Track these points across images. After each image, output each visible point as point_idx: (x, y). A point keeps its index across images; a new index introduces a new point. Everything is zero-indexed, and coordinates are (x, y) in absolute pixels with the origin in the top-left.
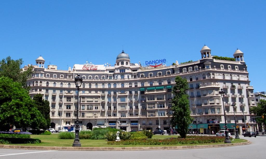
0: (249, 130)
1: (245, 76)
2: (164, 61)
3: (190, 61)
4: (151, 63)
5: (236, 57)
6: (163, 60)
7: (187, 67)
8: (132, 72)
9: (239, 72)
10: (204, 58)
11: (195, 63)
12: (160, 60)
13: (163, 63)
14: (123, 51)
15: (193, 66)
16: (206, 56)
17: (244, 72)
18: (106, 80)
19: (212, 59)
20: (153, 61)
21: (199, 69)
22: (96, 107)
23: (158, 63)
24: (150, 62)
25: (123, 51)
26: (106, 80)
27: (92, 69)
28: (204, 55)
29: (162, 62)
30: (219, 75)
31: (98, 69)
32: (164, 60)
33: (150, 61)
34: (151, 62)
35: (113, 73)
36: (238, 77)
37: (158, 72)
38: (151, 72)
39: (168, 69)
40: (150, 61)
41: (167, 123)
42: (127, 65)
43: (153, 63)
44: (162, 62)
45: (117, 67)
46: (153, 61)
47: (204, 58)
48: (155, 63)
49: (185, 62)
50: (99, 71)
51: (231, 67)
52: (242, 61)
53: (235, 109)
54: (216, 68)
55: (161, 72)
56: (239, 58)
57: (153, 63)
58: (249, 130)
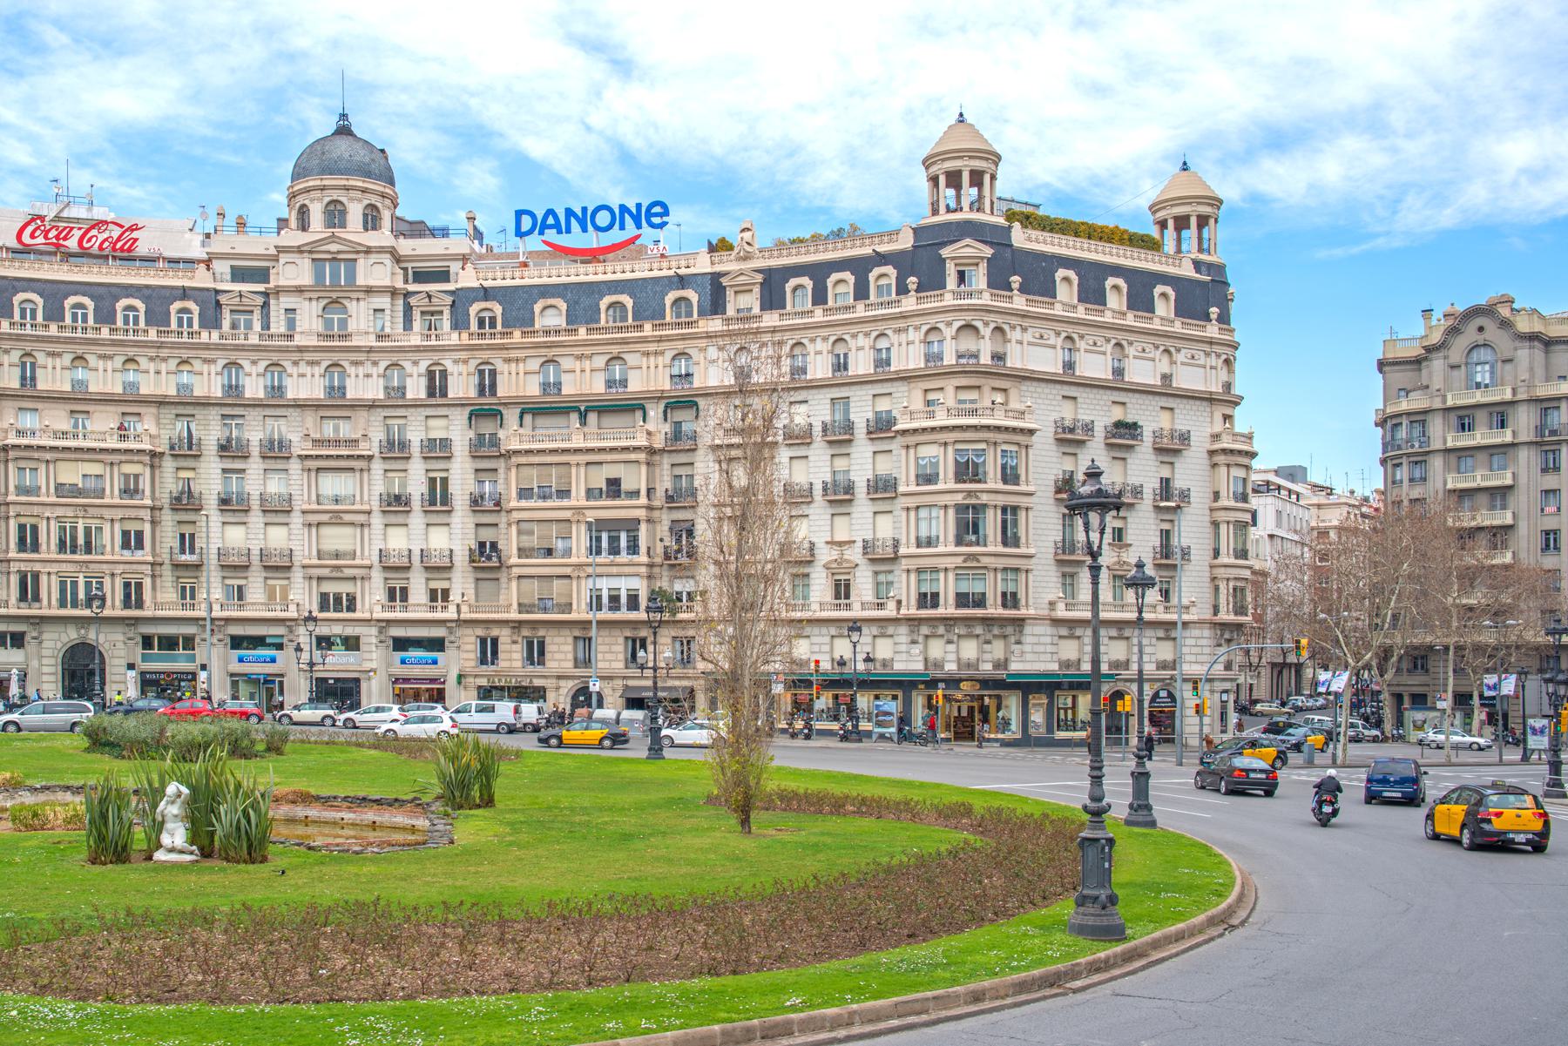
0: (1201, 725)
1: (1213, 361)
2: (656, 220)
3: (840, 230)
4: (557, 226)
5: (1171, 223)
7: (819, 272)
8: (412, 287)
9: (1178, 327)
10: (948, 210)
11: (882, 249)
13: (646, 230)
14: (344, 116)
15: (859, 267)
16: (958, 197)
17: (1212, 330)
18: (205, 335)
19: (1001, 221)
20: (569, 213)
21: (902, 290)
22: (126, 534)
23: (610, 227)
24: (551, 221)
25: (344, 116)
26: (205, 335)
28: (951, 192)
29: (639, 226)
31: (142, 249)
32: (657, 209)
33: (550, 212)
35: (261, 288)
36: (1164, 366)
38: (553, 296)
39: (682, 281)
40: (550, 212)
42: (374, 228)
44: (639, 226)
45: (293, 237)
47: (942, 209)
48: (585, 230)
49: (808, 236)
51: (1125, 290)
52: (1204, 257)
54: (1023, 289)
55: (628, 301)
56: (1185, 233)
58: (1201, 725)
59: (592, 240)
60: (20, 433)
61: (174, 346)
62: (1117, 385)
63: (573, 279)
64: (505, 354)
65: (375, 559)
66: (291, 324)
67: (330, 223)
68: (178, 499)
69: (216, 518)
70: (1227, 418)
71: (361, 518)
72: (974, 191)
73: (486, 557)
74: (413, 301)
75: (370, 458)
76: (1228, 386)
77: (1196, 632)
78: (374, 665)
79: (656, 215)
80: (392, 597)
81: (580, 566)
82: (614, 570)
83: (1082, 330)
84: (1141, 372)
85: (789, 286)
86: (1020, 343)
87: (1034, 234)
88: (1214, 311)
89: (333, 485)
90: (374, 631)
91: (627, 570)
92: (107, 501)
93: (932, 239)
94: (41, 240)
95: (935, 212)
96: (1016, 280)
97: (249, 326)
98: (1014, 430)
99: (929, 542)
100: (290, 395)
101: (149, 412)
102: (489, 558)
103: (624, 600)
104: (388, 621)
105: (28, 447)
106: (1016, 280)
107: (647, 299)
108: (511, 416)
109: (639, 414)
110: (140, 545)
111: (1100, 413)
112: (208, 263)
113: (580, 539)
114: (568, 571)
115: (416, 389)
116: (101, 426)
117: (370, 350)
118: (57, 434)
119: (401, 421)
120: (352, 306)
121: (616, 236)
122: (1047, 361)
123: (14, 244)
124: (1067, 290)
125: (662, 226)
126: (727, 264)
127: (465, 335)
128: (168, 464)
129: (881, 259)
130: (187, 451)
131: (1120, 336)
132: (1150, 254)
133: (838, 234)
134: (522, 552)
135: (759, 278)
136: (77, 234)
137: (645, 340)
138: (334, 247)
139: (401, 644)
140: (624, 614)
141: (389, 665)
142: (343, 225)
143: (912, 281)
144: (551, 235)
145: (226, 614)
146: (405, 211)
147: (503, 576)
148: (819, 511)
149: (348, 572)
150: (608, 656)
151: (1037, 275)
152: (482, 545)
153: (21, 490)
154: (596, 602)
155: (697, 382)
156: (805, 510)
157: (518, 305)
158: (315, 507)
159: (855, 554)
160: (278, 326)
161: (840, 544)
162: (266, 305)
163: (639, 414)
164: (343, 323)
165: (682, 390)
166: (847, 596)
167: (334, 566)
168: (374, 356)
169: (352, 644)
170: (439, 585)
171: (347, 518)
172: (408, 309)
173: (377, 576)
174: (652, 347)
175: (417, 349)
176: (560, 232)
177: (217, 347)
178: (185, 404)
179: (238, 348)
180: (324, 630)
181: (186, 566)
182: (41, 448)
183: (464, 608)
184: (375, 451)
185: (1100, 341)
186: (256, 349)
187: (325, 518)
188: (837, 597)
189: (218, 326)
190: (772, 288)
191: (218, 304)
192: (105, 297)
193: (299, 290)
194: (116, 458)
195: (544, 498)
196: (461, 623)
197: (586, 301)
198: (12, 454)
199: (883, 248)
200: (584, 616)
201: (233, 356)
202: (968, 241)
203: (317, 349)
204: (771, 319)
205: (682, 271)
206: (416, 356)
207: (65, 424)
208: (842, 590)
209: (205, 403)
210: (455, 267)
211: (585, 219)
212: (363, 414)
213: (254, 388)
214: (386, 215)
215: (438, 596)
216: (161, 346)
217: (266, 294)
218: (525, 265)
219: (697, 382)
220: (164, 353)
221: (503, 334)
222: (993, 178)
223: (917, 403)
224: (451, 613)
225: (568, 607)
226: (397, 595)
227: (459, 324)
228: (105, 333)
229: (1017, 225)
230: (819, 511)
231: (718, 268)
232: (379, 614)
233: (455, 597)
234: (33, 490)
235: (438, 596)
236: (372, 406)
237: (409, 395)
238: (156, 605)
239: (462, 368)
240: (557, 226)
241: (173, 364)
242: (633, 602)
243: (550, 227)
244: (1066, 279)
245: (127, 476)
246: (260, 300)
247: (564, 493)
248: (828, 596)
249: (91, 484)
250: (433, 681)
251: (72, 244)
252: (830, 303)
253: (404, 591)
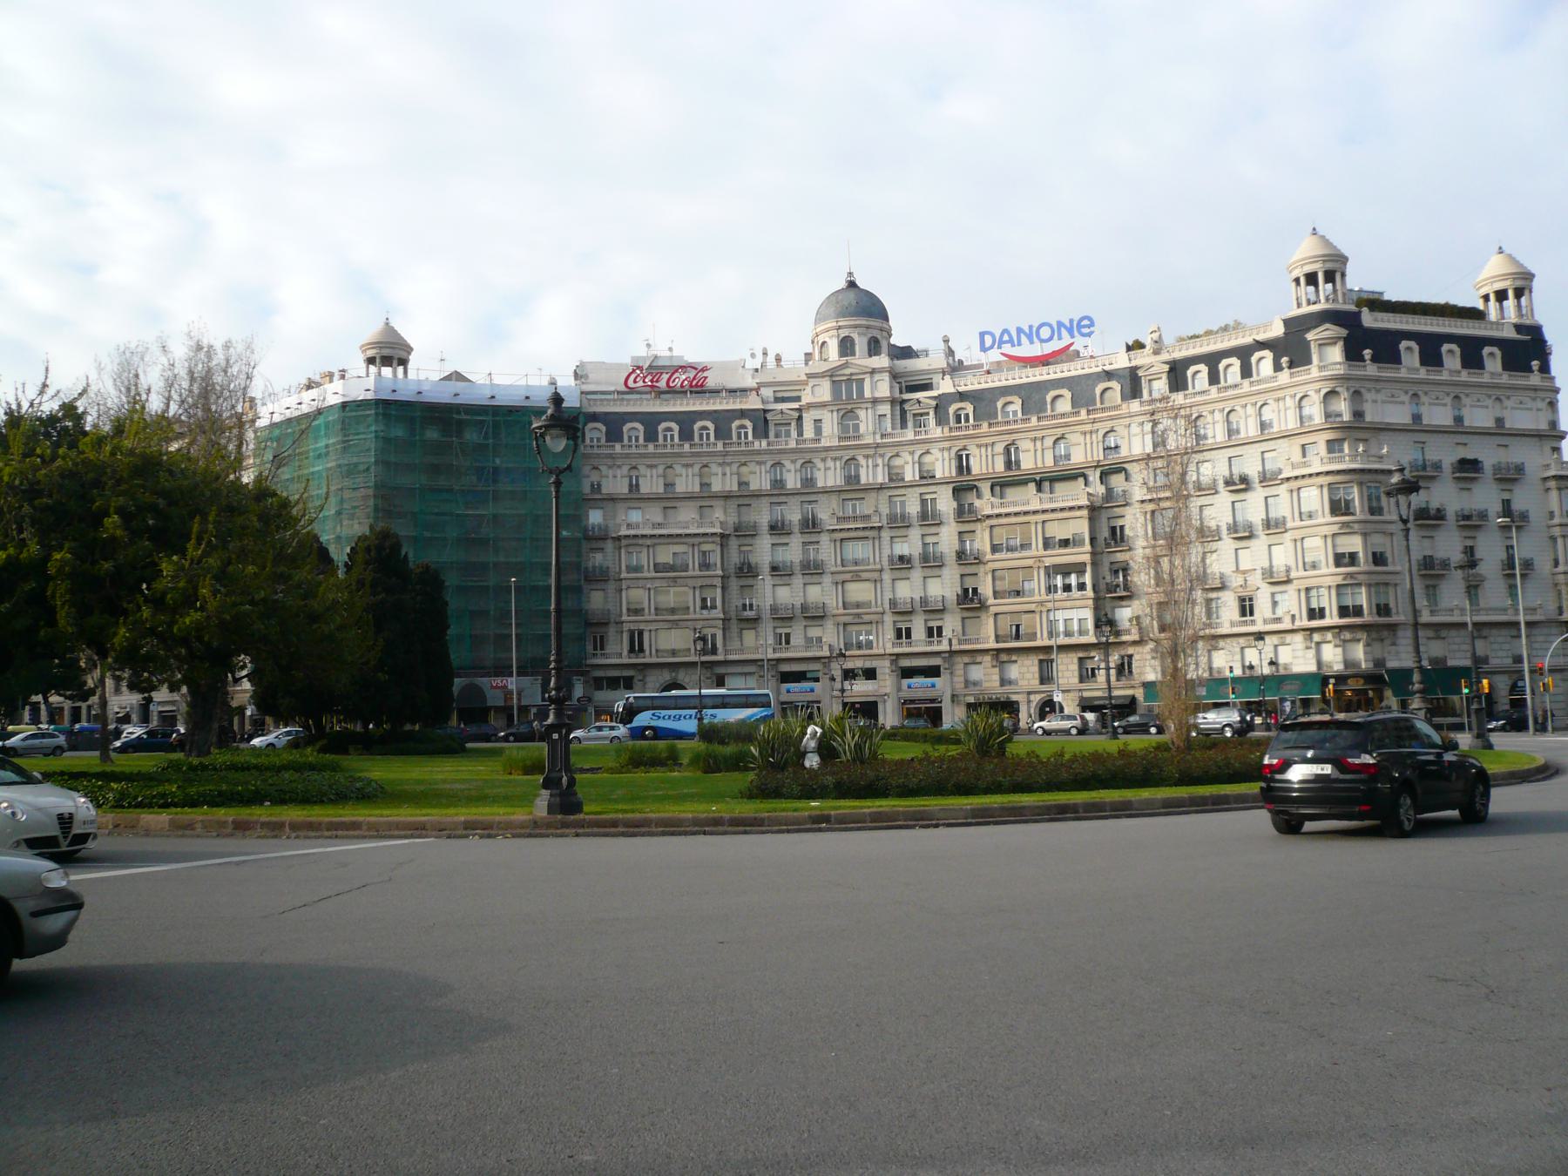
2: (1086, 331)
4: (1011, 341)
5: (1492, 297)
7: (1212, 360)
8: (907, 396)
10: (1309, 303)
12: (1060, 324)
14: (850, 274)
19: (1353, 308)
20: (1019, 330)
21: (1278, 367)
23: (1051, 338)
24: (1006, 338)
25: (850, 274)
26: (757, 443)
27: (678, 383)
28: (1311, 289)
30: (1392, 399)
32: (1086, 322)
33: (1006, 331)
35: (795, 405)
38: (1011, 394)
39: (1109, 375)
40: (1006, 331)
41: (1101, 676)
43: (1024, 339)
46: (1019, 330)
48: (1032, 342)
50: (715, 392)
53: (1473, 589)
54: (1374, 359)
57: (1024, 339)
59: (1036, 350)
60: (629, 526)
61: (736, 453)
62: (1459, 428)
63: (1025, 380)
64: (978, 441)
65: (887, 606)
66: (818, 431)
68: (741, 569)
69: (769, 581)
70: (1557, 450)
71: (876, 575)
72: (1330, 286)
73: (970, 600)
74: (907, 407)
75: (880, 528)
76: (1554, 424)
77: (1545, 631)
78: (888, 690)
80: (899, 636)
81: (1041, 603)
82: (1068, 604)
83: (1426, 388)
84: (1479, 417)
85: (1189, 373)
86: (1375, 401)
87: (1380, 315)
88: (1535, 364)
89: (857, 550)
90: (887, 663)
91: (1078, 603)
92: (690, 573)
93: (1297, 327)
95: (1299, 305)
96: (1367, 353)
97: (788, 434)
98: (1376, 471)
99: (1314, 566)
100: (820, 484)
101: (718, 503)
102: (972, 600)
104: (898, 655)
105: (635, 536)
106: (1367, 353)
107: (1082, 391)
108: (985, 488)
109: (1081, 480)
110: (714, 607)
111: (1446, 454)
112: (757, 390)
113: (1037, 584)
114: (1032, 607)
116: (686, 519)
117: (878, 446)
118: (654, 526)
120: (862, 414)
121: (1055, 345)
122: (1399, 415)
123: (623, 388)
124: (1410, 354)
125: (1089, 335)
126: (1141, 359)
127: (946, 429)
128: (734, 543)
129: (1261, 345)
130: (744, 532)
131: (1457, 390)
132: (1477, 323)
133: (1225, 329)
134: (996, 594)
135: (1166, 368)
136: (665, 377)
137: (1082, 423)
138: (848, 371)
139: (908, 673)
141: (899, 689)
142: (853, 354)
143: (1285, 360)
144: (1007, 349)
145: (777, 655)
146: (898, 340)
147: (984, 616)
148: (1227, 545)
149: (866, 618)
150: (1029, 676)
151: (1385, 347)
152: (966, 591)
153: (630, 569)
155: (1124, 452)
156: (1214, 546)
157: (984, 402)
158: (840, 569)
159: (1256, 580)
160: (809, 432)
161: (1244, 572)
162: (800, 418)
163: (1081, 480)
164: (856, 427)
165: (1113, 458)
166: (1252, 614)
167: (857, 616)
168: (881, 451)
169: (870, 674)
170: (934, 624)
171: (864, 575)
173: (889, 619)
174: (1088, 427)
175: (912, 443)
177: (766, 452)
178: (743, 497)
179: (781, 452)
180: (849, 665)
181: (748, 620)
182: (644, 536)
183: (954, 642)
184: (885, 522)
185: (1441, 395)
186: (793, 451)
187: (848, 577)
188: (1243, 614)
189: (766, 436)
190: (1177, 375)
191: (766, 421)
192: (686, 422)
193: (823, 405)
194: (696, 540)
196: (952, 653)
197: (1036, 397)
198: (624, 542)
199: (1261, 337)
200: (1046, 642)
201: (777, 458)
202: (1327, 326)
203: (839, 448)
204: (1179, 398)
205: (1107, 368)
206: (911, 448)
207: (659, 519)
208: (1246, 607)
209: (758, 495)
210: (936, 379)
211: (1032, 334)
212: (873, 494)
213: (792, 481)
214: (884, 344)
215: (933, 633)
216: (726, 454)
217: (799, 410)
218: (988, 372)
219: (1124, 452)
220: (729, 459)
221: (975, 427)
222: (1343, 275)
223: (1296, 456)
224: (944, 647)
225: (1033, 636)
226: (903, 634)
227: (941, 420)
228: (687, 447)
229: (1365, 310)
230: (1227, 545)
231: (1134, 364)
232: (890, 650)
233: (947, 632)
234: (638, 569)
235: (933, 633)
236: (881, 488)
238: (726, 652)
241: (734, 467)
244: (1409, 349)
245: (704, 553)
246: (796, 415)
248: (1236, 616)
249: (679, 562)
250: (933, 701)
251: (662, 384)
252: (1222, 383)
253: (908, 631)
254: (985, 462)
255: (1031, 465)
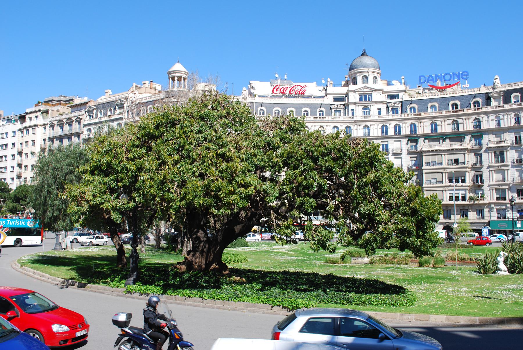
2: (465, 77)
4: (433, 80)
6: (462, 74)
12: (454, 74)
18: (327, 118)
23: (450, 80)
24: (431, 78)
32: (465, 74)
33: (430, 76)
34: (432, 77)
35: (343, 103)
37: (449, 101)
44: (459, 79)
46: (436, 76)
55: (458, 103)
67: (364, 83)
79: (464, 75)
94: (279, 92)
103: (460, 198)
115: (391, 132)
119: (386, 143)
138: (365, 90)
140: (461, 202)
142: (368, 82)
154: (451, 198)
172: (388, 107)
176: (434, 82)
191: (331, 109)
193: (355, 104)
195: (433, 165)
210: (401, 94)
237: (389, 134)
239: (404, 125)
240: (433, 80)
242: (464, 198)
243: (431, 80)
247: (441, 164)
251: (287, 93)
254: (424, 128)
255: (440, 132)
